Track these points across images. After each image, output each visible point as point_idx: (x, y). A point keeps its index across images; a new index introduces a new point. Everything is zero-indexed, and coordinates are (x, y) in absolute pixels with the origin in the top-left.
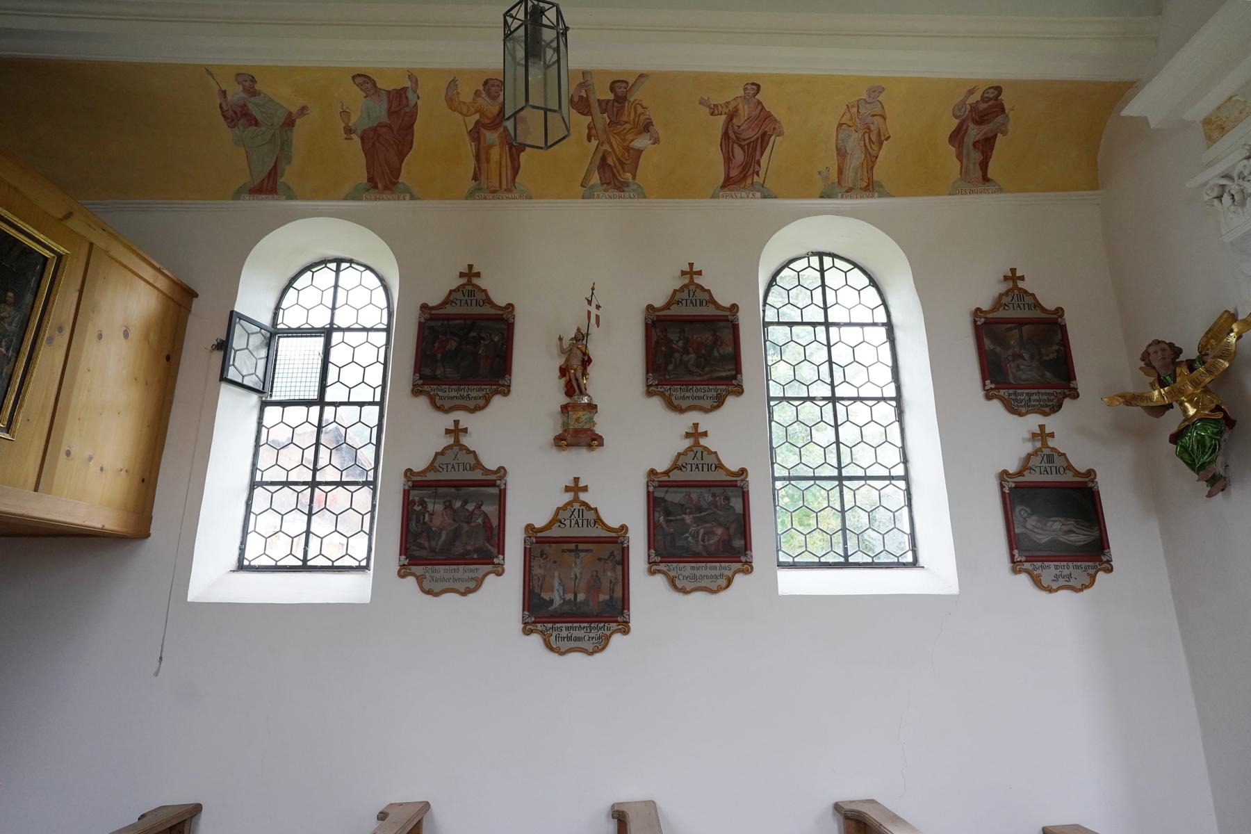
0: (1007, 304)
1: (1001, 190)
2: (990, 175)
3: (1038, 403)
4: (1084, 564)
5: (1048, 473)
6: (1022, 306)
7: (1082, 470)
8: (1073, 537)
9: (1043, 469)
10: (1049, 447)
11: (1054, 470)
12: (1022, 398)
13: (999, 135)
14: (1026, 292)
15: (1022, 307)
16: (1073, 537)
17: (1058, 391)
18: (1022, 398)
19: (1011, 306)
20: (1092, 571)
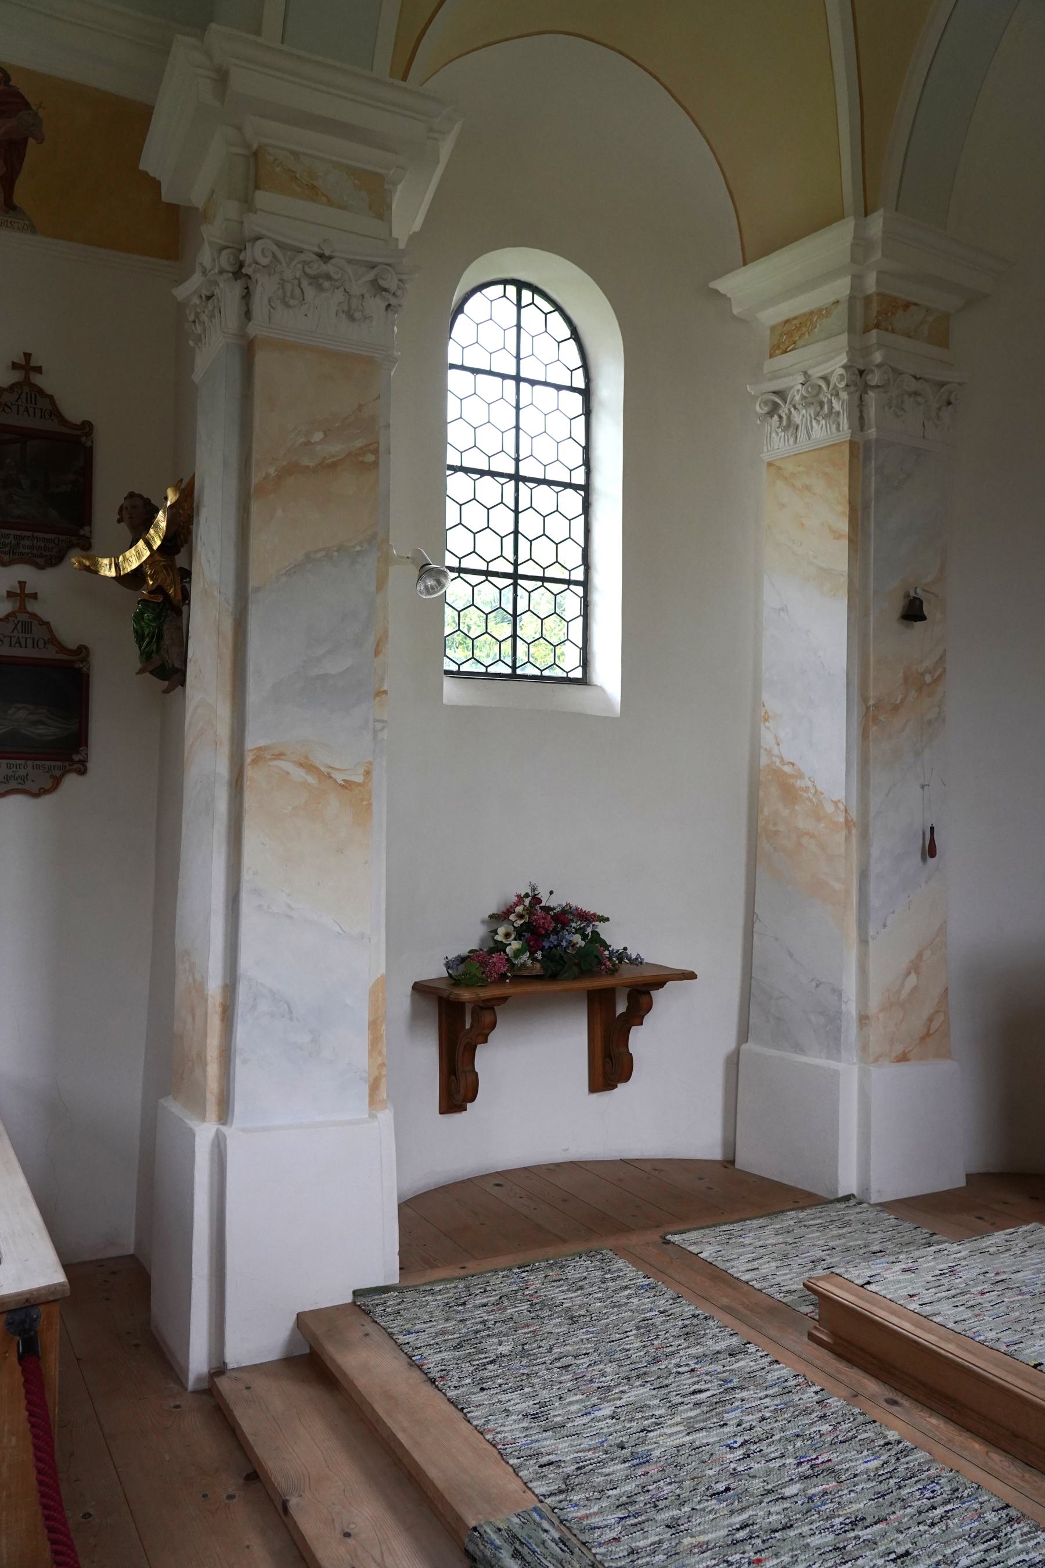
0: (10, 405)
1: (33, 229)
2: (17, 200)
3: (27, 551)
4: (48, 763)
5: (21, 646)
6: (31, 411)
7: (73, 646)
8: (41, 730)
9: (14, 640)
10: (27, 612)
11: (30, 641)
12: (7, 541)
13: (31, 141)
14: (41, 391)
15: (31, 411)
16: (41, 730)
17: (63, 537)
18: (7, 541)
19: (14, 408)
20: (57, 773)
